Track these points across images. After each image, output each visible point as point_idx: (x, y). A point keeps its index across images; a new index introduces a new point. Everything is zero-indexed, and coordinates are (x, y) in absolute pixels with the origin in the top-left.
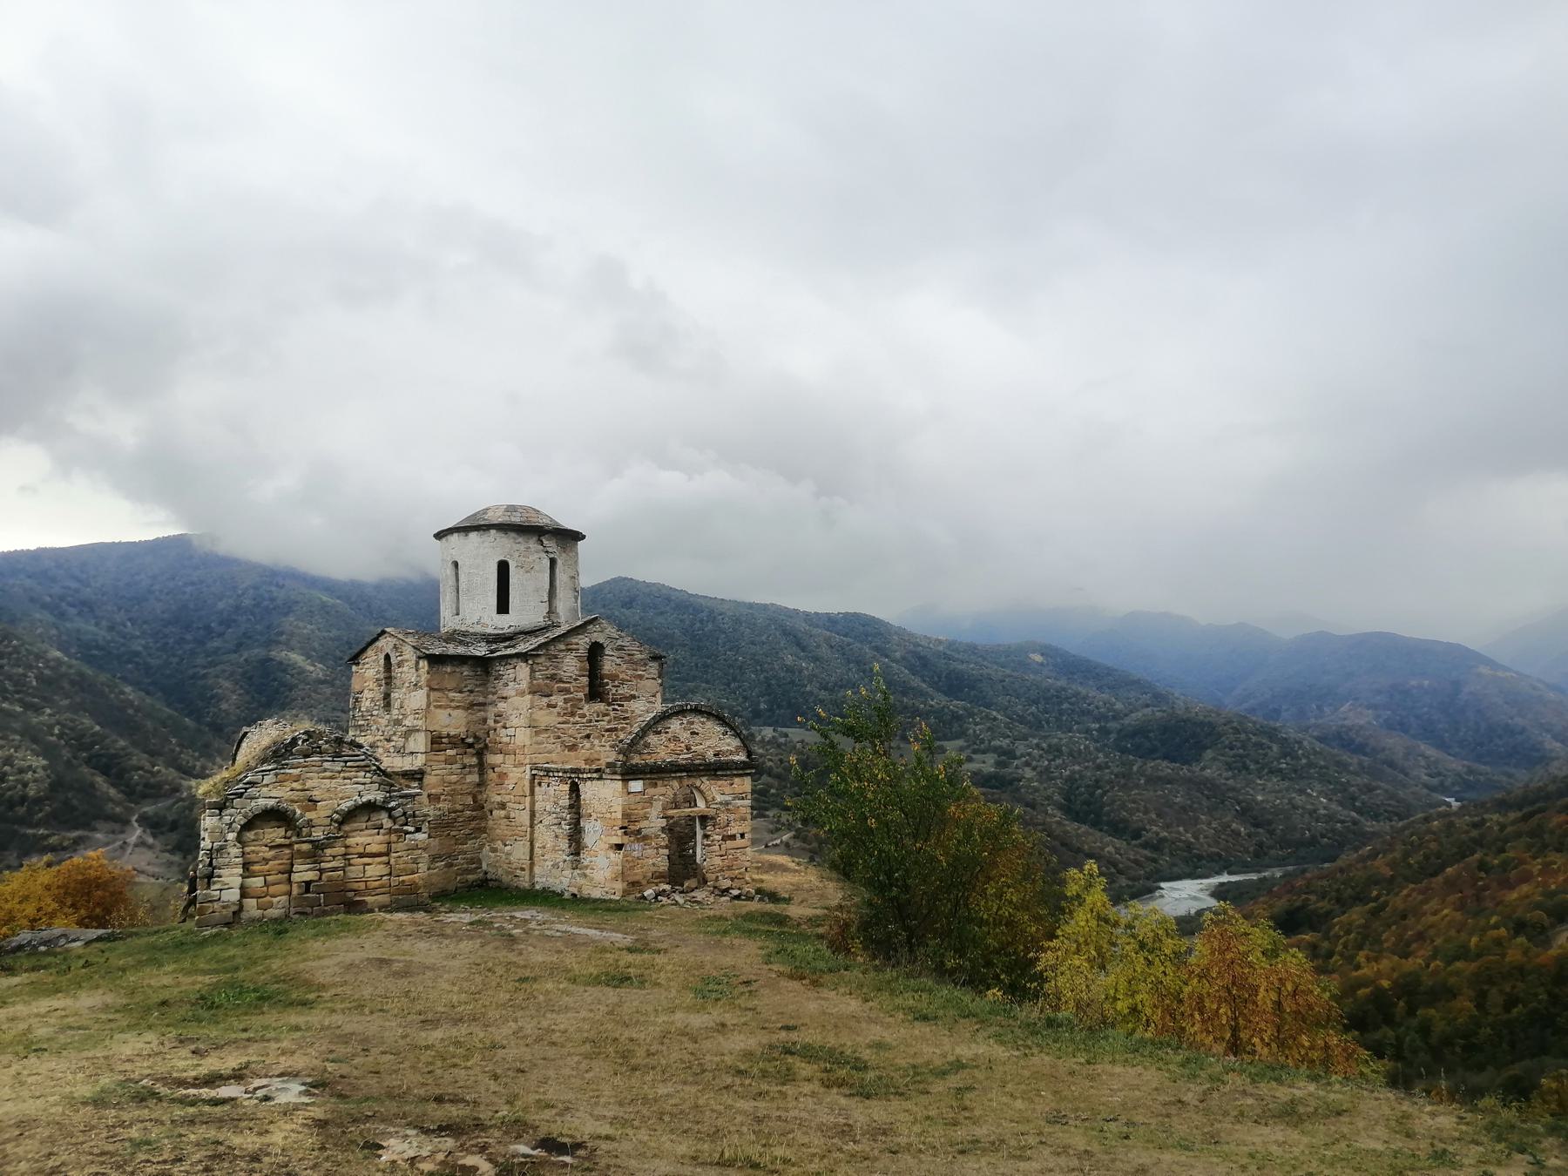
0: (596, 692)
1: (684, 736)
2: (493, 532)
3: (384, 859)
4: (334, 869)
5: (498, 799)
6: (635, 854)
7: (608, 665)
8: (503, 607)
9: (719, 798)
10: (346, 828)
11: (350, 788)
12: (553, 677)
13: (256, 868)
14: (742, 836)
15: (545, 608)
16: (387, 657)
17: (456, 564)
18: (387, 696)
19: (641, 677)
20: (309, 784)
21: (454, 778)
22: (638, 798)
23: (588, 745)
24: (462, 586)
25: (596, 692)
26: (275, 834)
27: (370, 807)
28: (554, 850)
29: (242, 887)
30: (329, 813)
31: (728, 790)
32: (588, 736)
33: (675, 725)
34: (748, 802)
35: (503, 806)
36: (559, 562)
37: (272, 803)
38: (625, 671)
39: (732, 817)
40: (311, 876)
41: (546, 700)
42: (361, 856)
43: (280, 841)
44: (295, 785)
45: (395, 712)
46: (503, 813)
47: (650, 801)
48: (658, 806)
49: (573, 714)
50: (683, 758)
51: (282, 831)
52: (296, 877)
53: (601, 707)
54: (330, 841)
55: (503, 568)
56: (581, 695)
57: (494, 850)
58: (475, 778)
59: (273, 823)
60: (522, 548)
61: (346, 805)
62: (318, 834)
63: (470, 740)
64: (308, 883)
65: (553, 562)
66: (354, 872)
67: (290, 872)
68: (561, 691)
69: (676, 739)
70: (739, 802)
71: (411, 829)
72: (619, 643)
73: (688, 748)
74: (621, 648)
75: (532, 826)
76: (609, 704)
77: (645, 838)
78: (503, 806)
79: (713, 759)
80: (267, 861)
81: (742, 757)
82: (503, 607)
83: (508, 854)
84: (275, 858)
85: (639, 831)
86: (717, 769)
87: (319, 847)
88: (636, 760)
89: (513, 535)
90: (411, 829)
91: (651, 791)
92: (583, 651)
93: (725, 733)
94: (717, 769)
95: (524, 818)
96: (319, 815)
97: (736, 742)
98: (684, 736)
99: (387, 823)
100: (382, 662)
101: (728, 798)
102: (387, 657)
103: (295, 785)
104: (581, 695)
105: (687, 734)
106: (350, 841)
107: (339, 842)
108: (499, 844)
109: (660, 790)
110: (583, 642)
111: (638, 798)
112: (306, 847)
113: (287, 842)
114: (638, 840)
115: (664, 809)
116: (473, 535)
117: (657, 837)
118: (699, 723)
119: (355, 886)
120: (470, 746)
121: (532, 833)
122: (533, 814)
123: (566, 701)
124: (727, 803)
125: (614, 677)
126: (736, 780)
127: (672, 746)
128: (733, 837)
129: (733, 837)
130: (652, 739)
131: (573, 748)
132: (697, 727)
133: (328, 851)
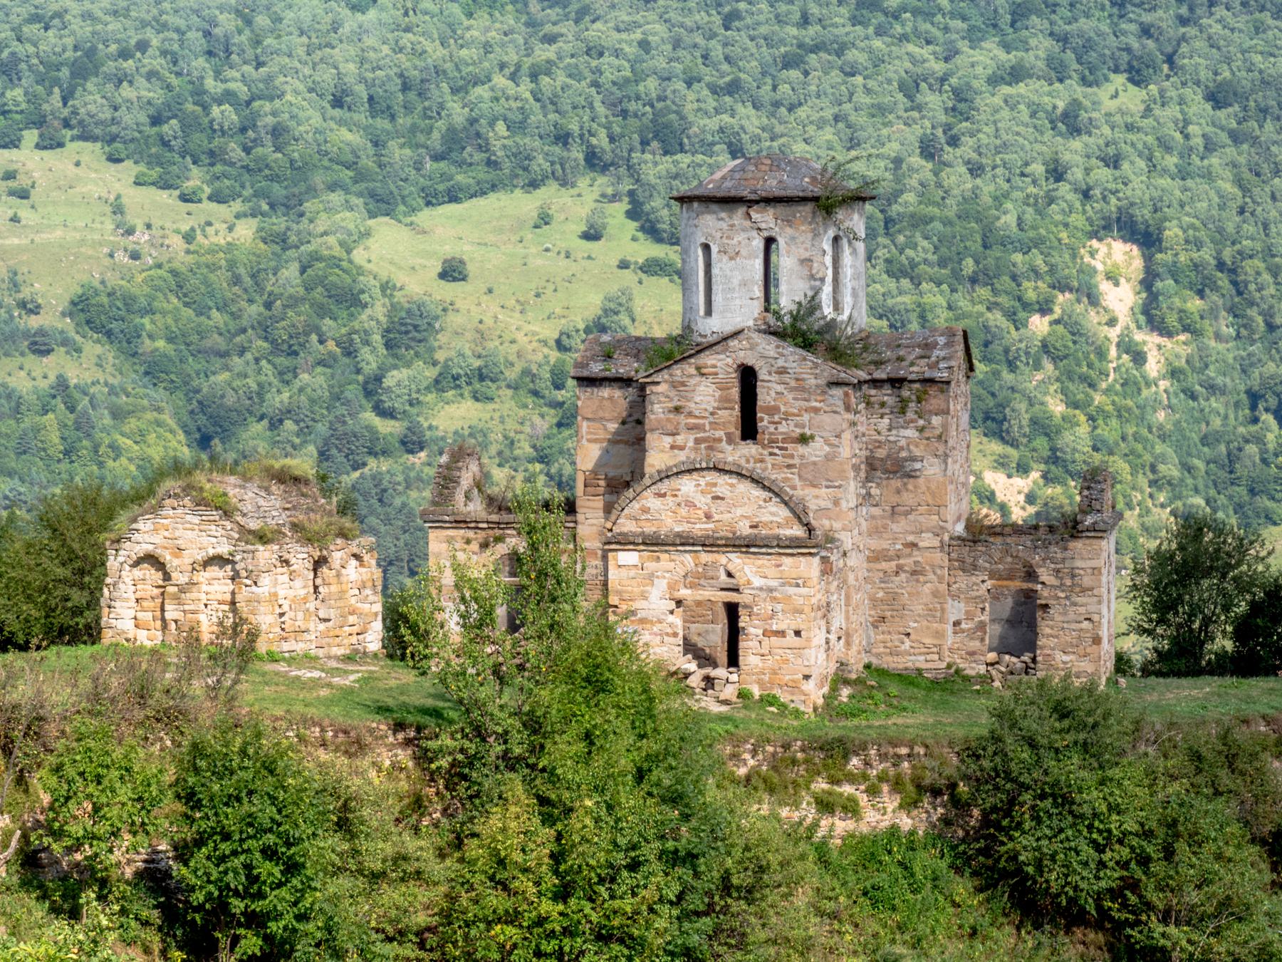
1: (703, 501)
2: (696, 205)
7: (765, 397)
9: (757, 582)
11: (205, 540)
12: (677, 410)
15: (758, 306)
19: (816, 410)
20: (177, 534)
22: (632, 573)
31: (772, 572)
33: (687, 486)
37: (151, 547)
38: (791, 402)
39: (779, 607)
41: (669, 439)
47: (651, 577)
48: (661, 585)
50: (700, 528)
53: (750, 449)
54: (192, 584)
60: (724, 225)
61: (200, 556)
65: (770, 241)
68: (691, 428)
69: (691, 504)
72: (781, 363)
73: (708, 516)
74: (782, 371)
76: (764, 446)
81: (798, 531)
87: (182, 590)
89: (714, 207)
91: (651, 565)
97: (784, 513)
101: (774, 583)
104: (720, 434)
110: (722, 364)
111: (632, 573)
115: (672, 587)
118: (724, 484)
123: (697, 441)
124: (771, 590)
125: (772, 410)
126: (787, 561)
127: (683, 511)
128: (782, 634)
129: (782, 634)
132: (719, 491)
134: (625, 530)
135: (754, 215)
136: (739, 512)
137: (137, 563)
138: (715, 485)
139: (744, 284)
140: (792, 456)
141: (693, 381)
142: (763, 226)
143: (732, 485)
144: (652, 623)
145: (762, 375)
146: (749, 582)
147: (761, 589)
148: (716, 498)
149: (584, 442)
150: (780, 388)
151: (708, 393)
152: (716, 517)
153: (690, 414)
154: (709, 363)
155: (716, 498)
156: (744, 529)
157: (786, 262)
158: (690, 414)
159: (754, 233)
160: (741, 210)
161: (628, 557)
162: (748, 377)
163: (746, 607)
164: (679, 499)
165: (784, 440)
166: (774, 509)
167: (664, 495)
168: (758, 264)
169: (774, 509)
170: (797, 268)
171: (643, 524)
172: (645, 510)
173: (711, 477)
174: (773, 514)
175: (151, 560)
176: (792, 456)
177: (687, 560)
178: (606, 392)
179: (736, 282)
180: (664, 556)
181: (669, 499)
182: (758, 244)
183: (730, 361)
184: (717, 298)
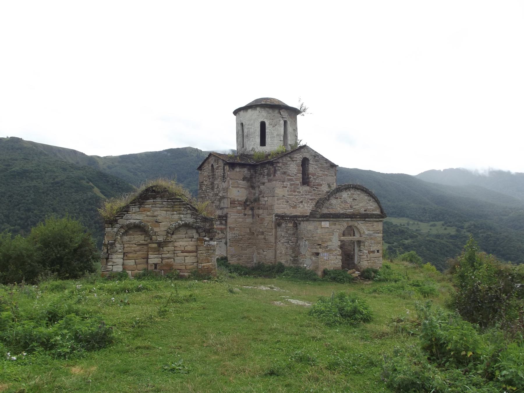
0: (305, 181)
1: (349, 200)
2: (258, 109)
3: (195, 254)
4: (168, 258)
5: (261, 230)
6: (325, 258)
8: (263, 143)
9: (367, 232)
10: (174, 236)
13: (130, 255)
14: (378, 251)
16: (212, 166)
17: (242, 124)
18: (212, 183)
19: (327, 175)
20: (156, 213)
21: (241, 220)
22: (326, 230)
23: (302, 206)
24: (245, 134)
25: (305, 181)
26: (140, 238)
27: (187, 226)
28: (286, 254)
29: (123, 265)
30: (166, 229)
31: (371, 229)
32: (302, 202)
33: (345, 195)
34: (381, 235)
35: (263, 233)
36: (289, 122)
37: (137, 222)
40: (157, 261)
42: (183, 252)
43: (143, 242)
44: (148, 213)
45: (216, 190)
46: (263, 237)
48: (336, 234)
49: (294, 191)
50: (350, 211)
51: (143, 237)
52: (150, 261)
53: (307, 188)
55: (263, 125)
56: (298, 182)
57: (259, 254)
58: (249, 220)
59: (139, 233)
62: (160, 239)
63: (248, 203)
64: (156, 265)
65: (285, 122)
66: (179, 260)
67: (147, 258)
68: (289, 180)
69: (346, 202)
70: (377, 235)
71: (207, 239)
75: (276, 243)
76: (311, 187)
77: (330, 250)
78: (263, 233)
79: (364, 212)
80: (136, 252)
81: (378, 212)
82: (263, 143)
83: (265, 256)
84: (140, 251)
85: (327, 247)
86: (365, 217)
87: (161, 245)
88: (325, 211)
89: (267, 109)
90: (207, 239)
91: (333, 227)
92: (299, 162)
93: (370, 200)
94: (365, 217)
95: (272, 240)
96: (161, 230)
98: (349, 200)
99: (196, 236)
100: (210, 168)
101: (371, 232)
102: (212, 166)
103: (148, 213)
104: (298, 182)
105: (351, 200)
106: (176, 244)
107: (170, 245)
108: (261, 251)
109: (338, 226)
112: (155, 245)
113: (146, 243)
114: (327, 251)
115: (340, 236)
116: (250, 111)
117: (336, 250)
118: (357, 194)
119: (180, 267)
120: (248, 205)
121: (276, 246)
122: (276, 238)
123: (291, 185)
125: (314, 175)
126: (375, 224)
128: (373, 252)
129: (373, 252)
130: (333, 201)
131: (295, 207)
132: (355, 196)
133: (165, 249)
134: (324, 212)
135: (282, 113)
136: (361, 205)
137: (126, 233)
138: (353, 194)
139: (278, 135)
140: (320, 191)
141: (289, 163)
142: (284, 116)
143: (359, 194)
144: (333, 251)
145: (311, 162)
146: (364, 233)
147: (368, 235)
148: (354, 199)
149: (230, 187)
150: (316, 167)
151: (293, 168)
152: (354, 207)
153: (289, 175)
154: (295, 156)
155: (354, 199)
156: (362, 211)
157: (290, 129)
158: (289, 175)
159: (281, 119)
160: (277, 111)
161: (326, 224)
162: (305, 162)
163: (363, 242)
164: (342, 200)
165: (317, 185)
166: (371, 204)
167: (337, 198)
168: (282, 128)
169: (371, 204)
170: (293, 132)
171: (330, 210)
172: (331, 204)
173: (352, 191)
174: (371, 206)
175: (139, 228)
176: (320, 191)
177: (343, 225)
178: (237, 169)
179: (275, 134)
180: (337, 223)
181: (339, 200)
182: (282, 122)
183: (301, 156)
184: (268, 140)
